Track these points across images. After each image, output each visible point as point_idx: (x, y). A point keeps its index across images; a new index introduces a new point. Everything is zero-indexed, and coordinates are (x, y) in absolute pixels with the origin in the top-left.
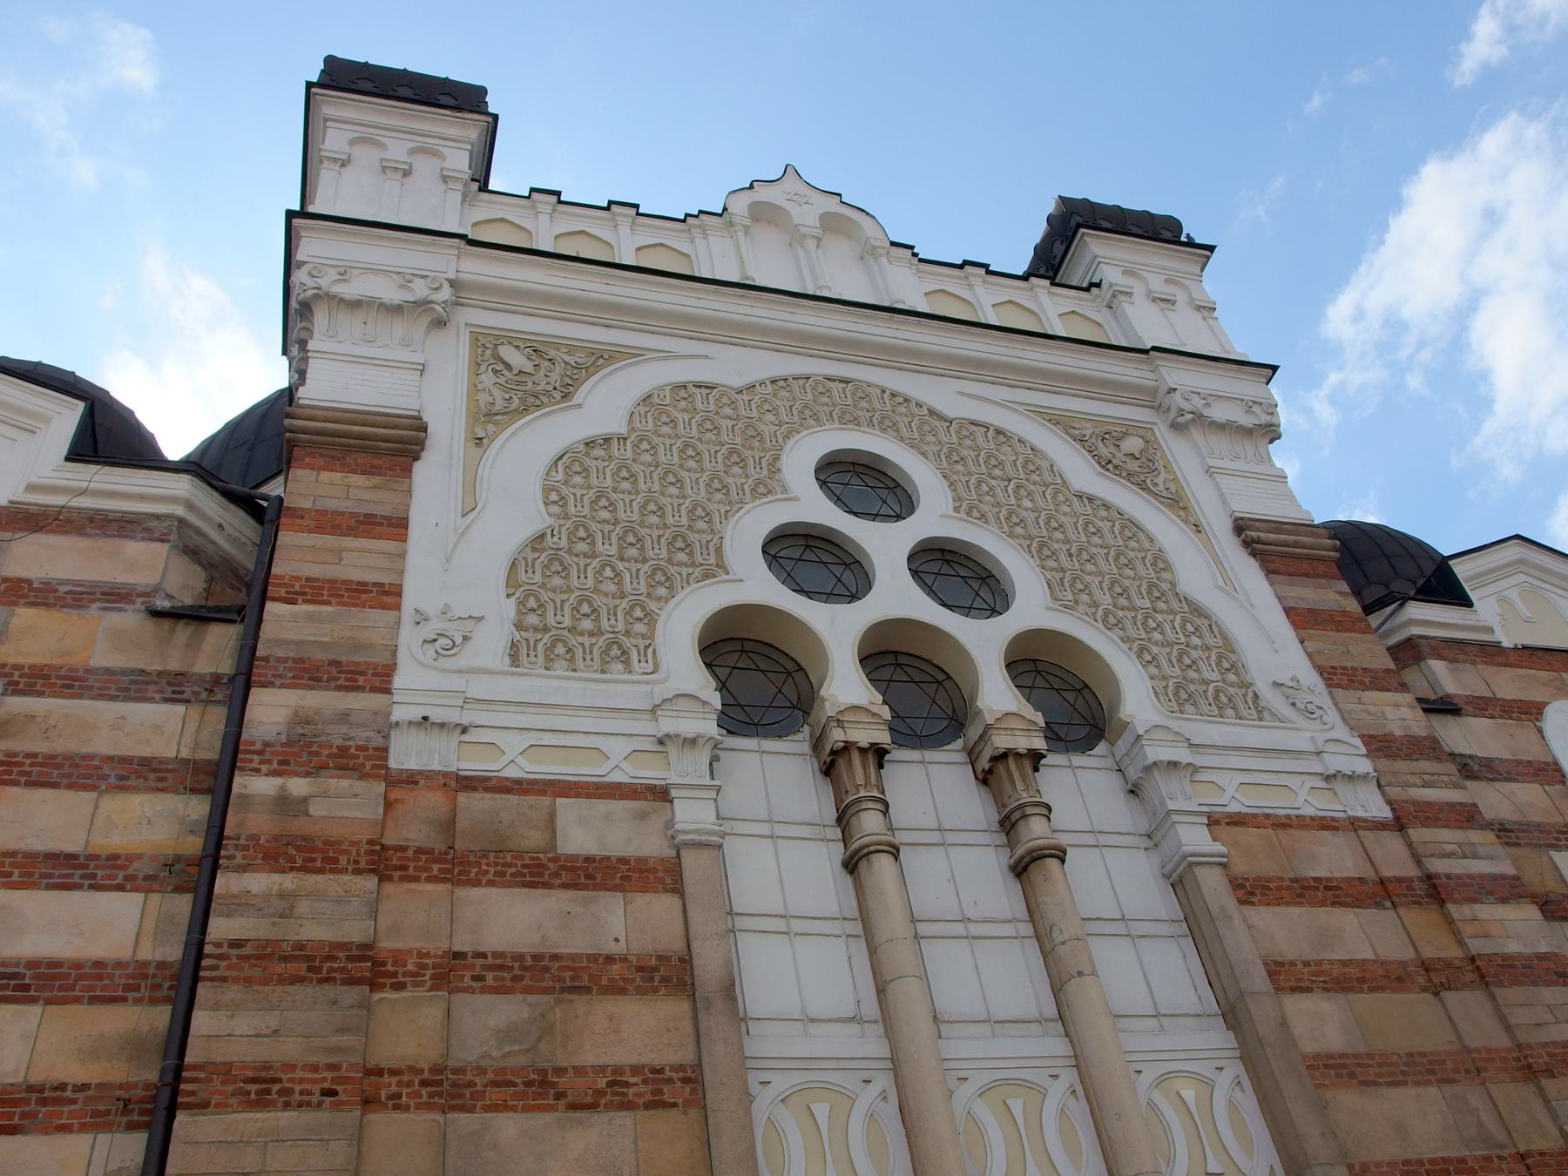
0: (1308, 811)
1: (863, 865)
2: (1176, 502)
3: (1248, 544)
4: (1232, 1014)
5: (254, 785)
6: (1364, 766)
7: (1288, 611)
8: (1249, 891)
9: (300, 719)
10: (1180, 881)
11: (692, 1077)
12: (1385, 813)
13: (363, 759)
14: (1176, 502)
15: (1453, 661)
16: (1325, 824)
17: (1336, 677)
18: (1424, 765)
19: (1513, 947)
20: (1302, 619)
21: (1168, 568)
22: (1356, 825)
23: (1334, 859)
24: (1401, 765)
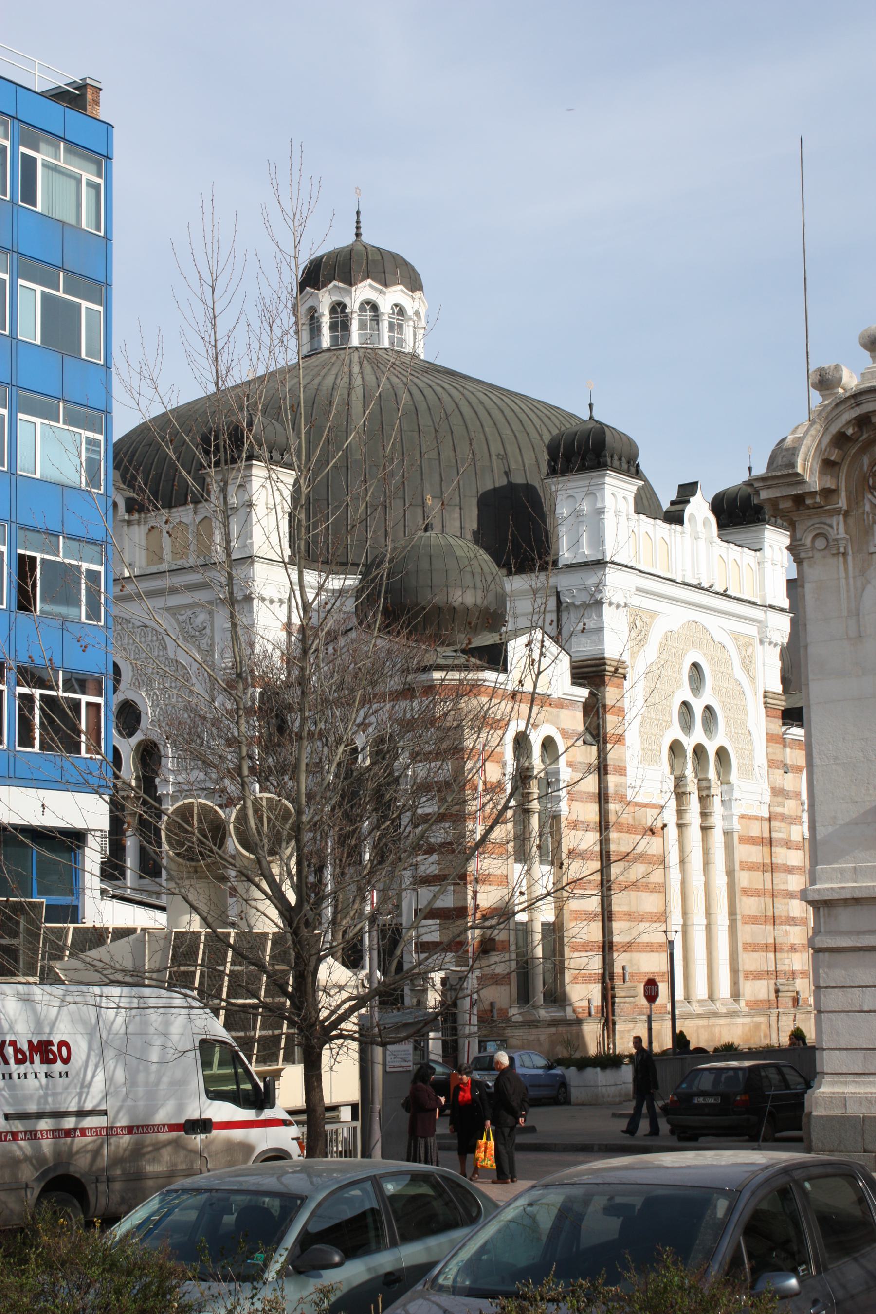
0: (755, 814)
1: (684, 828)
2: (753, 679)
3: (765, 703)
4: (730, 873)
5: (612, 807)
6: (767, 798)
7: (767, 734)
8: (743, 840)
9: (616, 786)
10: (727, 834)
11: (664, 885)
12: (767, 815)
13: (622, 798)
14: (753, 679)
15: (792, 748)
16: (756, 818)
17: (772, 764)
18: (780, 799)
19: (780, 862)
20: (771, 738)
21: (746, 715)
22: (762, 819)
23: (756, 830)
24: (776, 799)
